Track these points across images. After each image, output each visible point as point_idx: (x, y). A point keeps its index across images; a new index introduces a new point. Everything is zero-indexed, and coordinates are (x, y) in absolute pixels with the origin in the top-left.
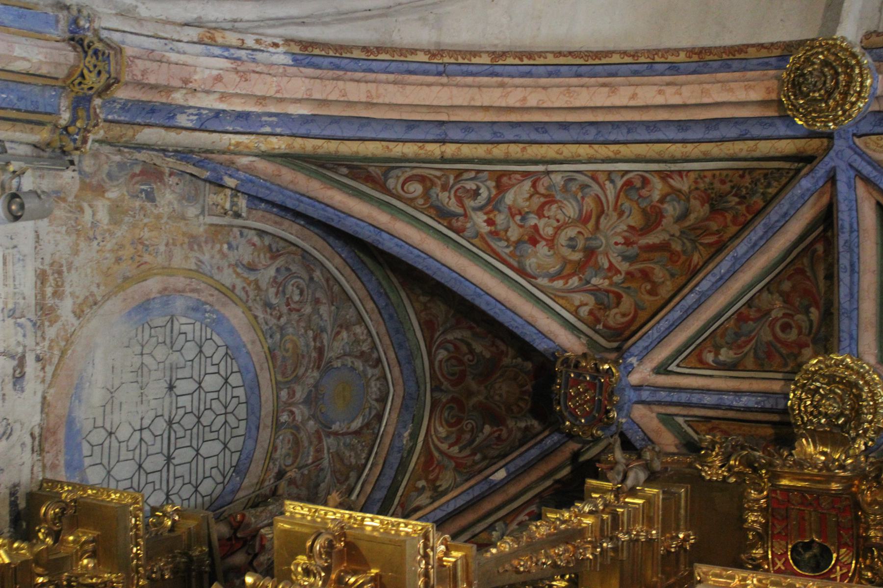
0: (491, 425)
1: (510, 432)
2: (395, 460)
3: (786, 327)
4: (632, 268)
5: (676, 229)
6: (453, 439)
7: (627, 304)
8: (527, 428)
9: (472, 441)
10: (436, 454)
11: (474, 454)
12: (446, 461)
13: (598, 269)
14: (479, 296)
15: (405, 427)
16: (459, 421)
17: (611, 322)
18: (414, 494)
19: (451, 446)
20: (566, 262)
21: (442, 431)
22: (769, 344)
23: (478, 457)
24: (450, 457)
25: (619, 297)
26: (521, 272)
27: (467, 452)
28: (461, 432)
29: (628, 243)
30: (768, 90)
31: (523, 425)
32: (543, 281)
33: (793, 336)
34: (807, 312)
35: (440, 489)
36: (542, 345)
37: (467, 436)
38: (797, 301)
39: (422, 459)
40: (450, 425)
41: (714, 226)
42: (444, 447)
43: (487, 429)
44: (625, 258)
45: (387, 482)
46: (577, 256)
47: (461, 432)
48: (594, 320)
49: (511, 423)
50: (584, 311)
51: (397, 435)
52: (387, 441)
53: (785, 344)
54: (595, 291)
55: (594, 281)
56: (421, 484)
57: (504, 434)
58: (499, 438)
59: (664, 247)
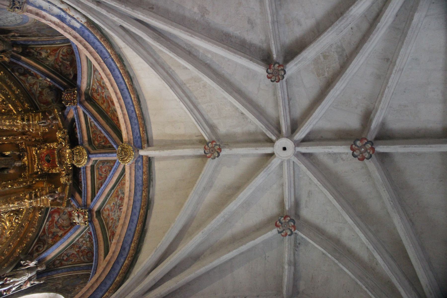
0: (70, 64)
1: (69, 70)
2: (52, 42)
3: (100, 137)
4: (105, 99)
5: (113, 109)
6: (64, 54)
7: (98, 97)
8: (71, 74)
9: (64, 60)
10: (58, 51)
11: (61, 62)
12: (57, 55)
13: (102, 89)
14: (79, 67)
15: (60, 42)
16: (68, 54)
17: (94, 94)
18: (45, 51)
19: (62, 54)
20: (100, 81)
21: (65, 50)
22: (96, 134)
23: (60, 64)
24: (58, 56)
25: (99, 95)
26: (94, 71)
27: (61, 60)
28: (66, 56)
29: (108, 97)
30: (126, 139)
31: (71, 73)
32: (95, 77)
33: (99, 139)
34: (103, 142)
35: (48, 58)
36: (78, 83)
37: (65, 58)
38: (104, 139)
39: (55, 48)
40: (67, 52)
41: (115, 118)
42: (61, 53)
43: (68, 63)
44: (105, 96)
45: (44, 43)
46: (102, 84)
47: (66, 56)
48: (93, 89)
49: (71, 69)
50: (94, 87)
51: (57, 41)
52: (54, 39)
53: (97, 137)
54: (98, 89)
55: (99, 89)
56: (49, 51)
57: (68, 69)
58: (67, 67)
59: (110, 106)
